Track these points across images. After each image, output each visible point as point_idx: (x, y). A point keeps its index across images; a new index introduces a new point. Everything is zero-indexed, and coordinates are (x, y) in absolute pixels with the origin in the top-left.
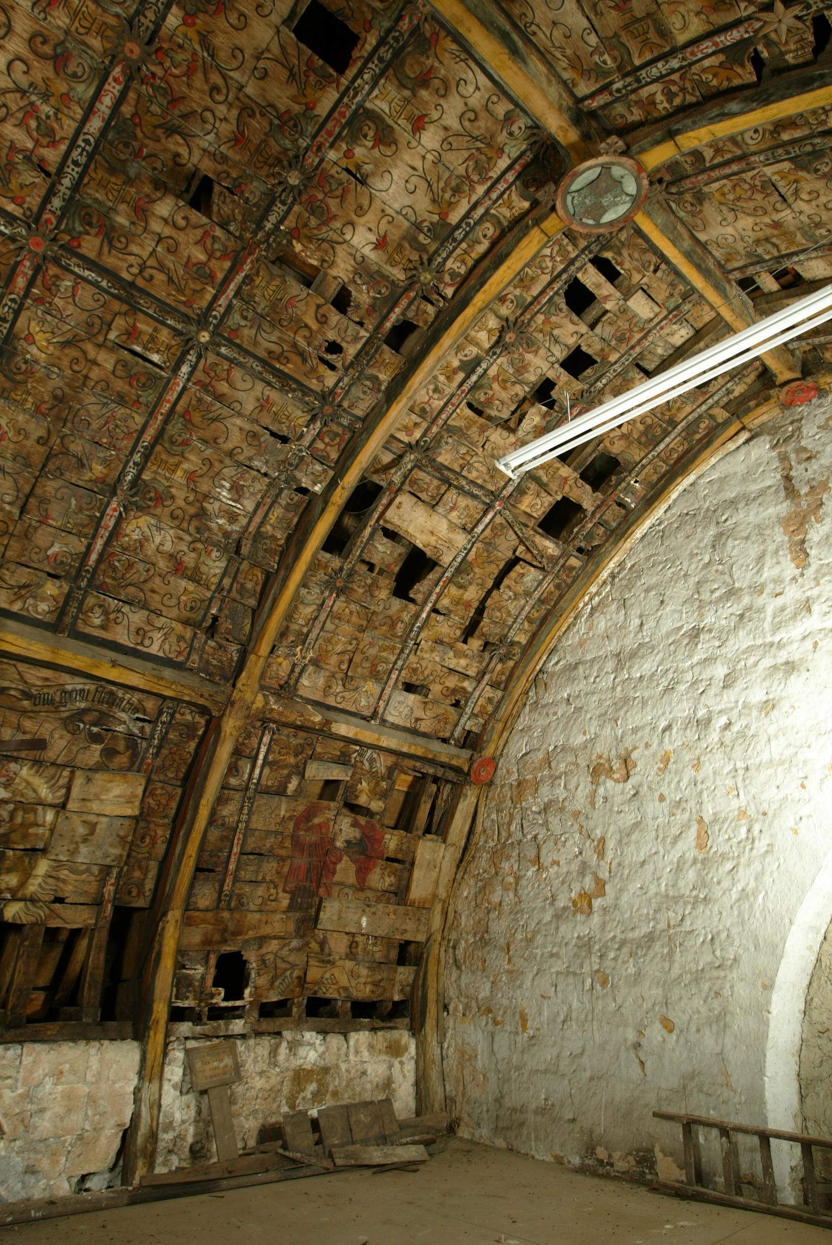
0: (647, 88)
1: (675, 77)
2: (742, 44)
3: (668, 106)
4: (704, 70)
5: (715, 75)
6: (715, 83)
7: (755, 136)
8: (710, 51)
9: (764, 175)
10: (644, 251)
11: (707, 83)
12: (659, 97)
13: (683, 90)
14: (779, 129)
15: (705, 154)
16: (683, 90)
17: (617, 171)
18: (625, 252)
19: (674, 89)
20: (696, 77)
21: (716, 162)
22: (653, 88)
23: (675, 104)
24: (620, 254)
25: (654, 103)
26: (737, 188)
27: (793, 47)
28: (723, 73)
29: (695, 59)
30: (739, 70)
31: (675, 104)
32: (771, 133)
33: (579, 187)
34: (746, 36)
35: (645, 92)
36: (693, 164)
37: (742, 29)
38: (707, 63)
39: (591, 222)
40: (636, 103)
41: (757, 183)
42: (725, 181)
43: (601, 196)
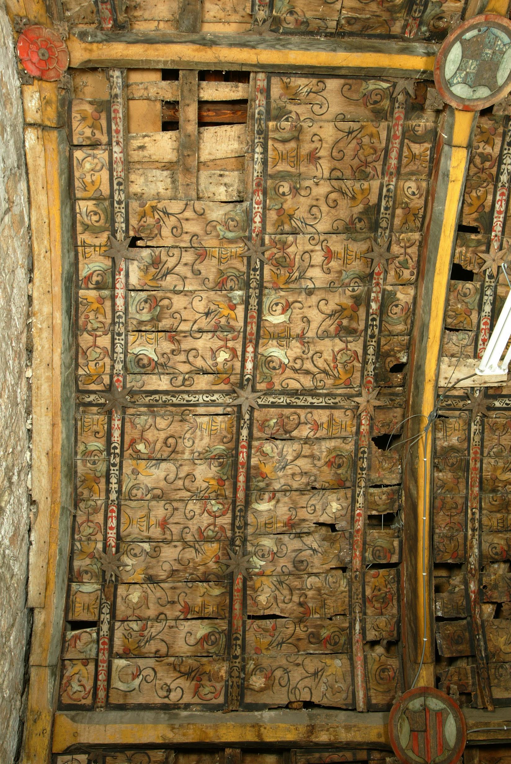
0: (499, 145)
1: (494, 171)
2: (489, 228)
3: (478, 151)
4: (486, 193)
5: (478, 197)
6: (474, 194)
7: (410, 191)
8: (497, 206)
9: (373, 178)
10: (366, 27)
11: (476, 189)
12: (488, 149)
13: (483, 170)
14: (407, 211)
15: (417, 146)
16: (483, 170)
17: (483, 92)
18: (385, 16)
19: (487, 164)
20: (485, 184)
21: (405, 149)
22: (497, 149)
23: (477, 157)
24: (388, 10)
25: (487, 142)
26: (372, 151)
27: (469, 255)
28: (477, 203)
29: (498, 193)
30: (474, 216)
31: (477, 157)
32: (406, 203)
33: (505, 56)
34: (493, 234)
35: (498, 141)
36: (414, 130)
37: (499, 234)
38: (490, 198)
39: (468, 35)
40: (496, 129)
41: (369, 170)
42: (384, 145)
43: (479, 65)
